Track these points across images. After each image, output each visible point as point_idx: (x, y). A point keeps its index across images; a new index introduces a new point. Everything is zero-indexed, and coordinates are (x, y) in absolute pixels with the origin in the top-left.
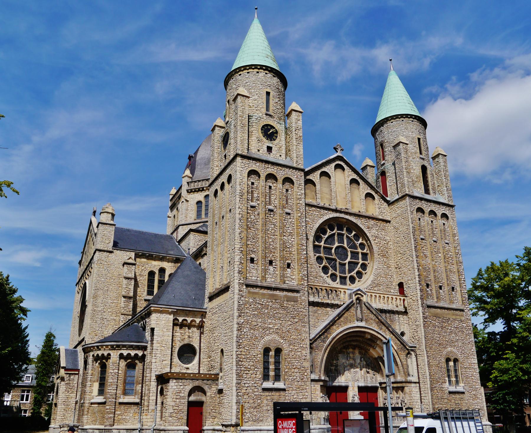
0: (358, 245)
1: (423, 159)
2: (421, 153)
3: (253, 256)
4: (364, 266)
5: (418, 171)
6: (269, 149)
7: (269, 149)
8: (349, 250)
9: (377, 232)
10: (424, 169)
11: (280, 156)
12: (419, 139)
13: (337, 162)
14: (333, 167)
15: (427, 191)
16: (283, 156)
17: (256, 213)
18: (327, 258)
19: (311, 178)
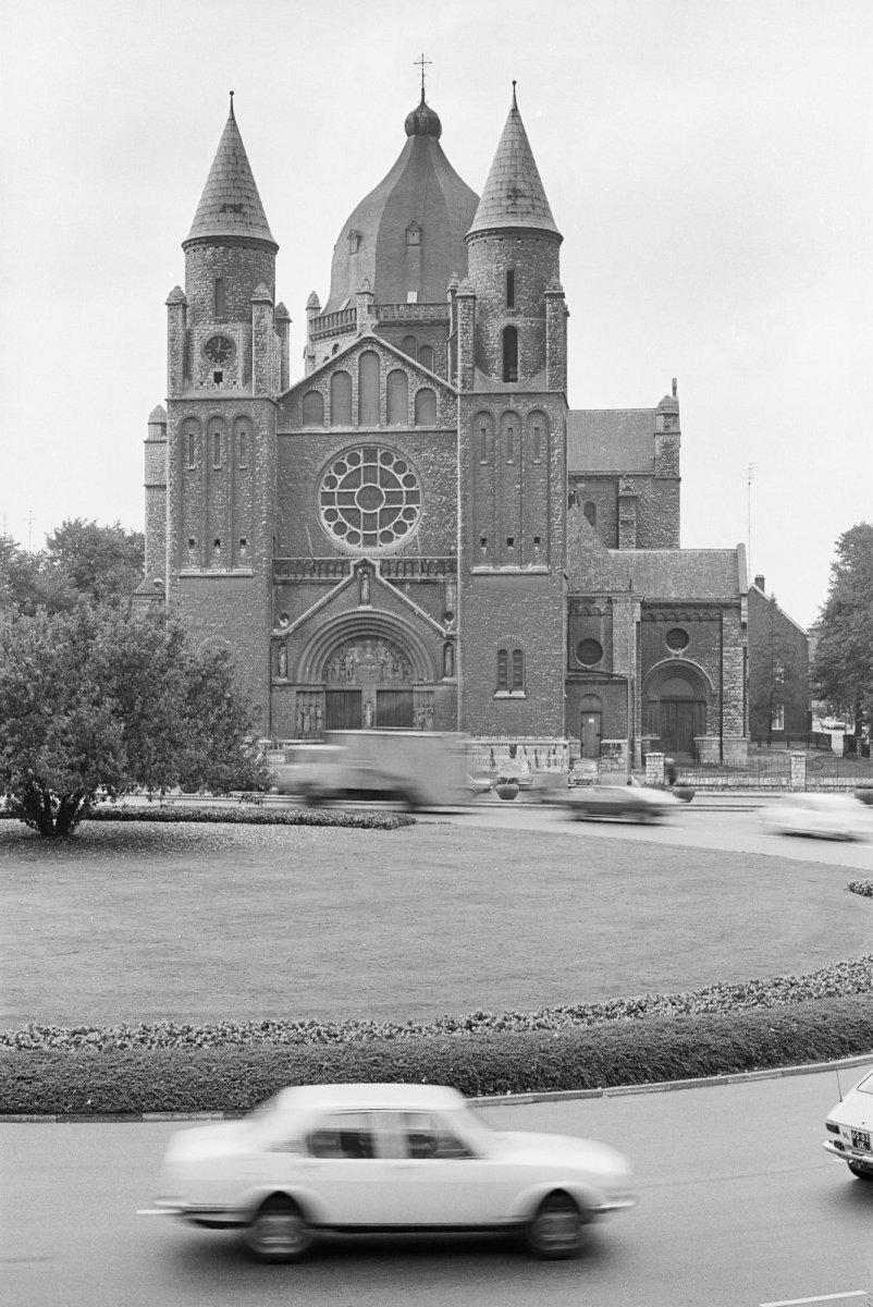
0: (401, 481)
1: (514, 315)
2: (510, 303)
3: (193, 537)
4: (409, 514)
5: (495, 342)
6: (218, 377)
7: (218, 377)
8: (383, 490)
9: (432, 455)
10: (510, 334)
11: (235, 383)
12: (510, 275)
13: (365, 349)
14: (357, 359)
15: (508, 377)
16: (239, 382)
17: (196, 478)
18: (340, 509)
19: (315, 388)
